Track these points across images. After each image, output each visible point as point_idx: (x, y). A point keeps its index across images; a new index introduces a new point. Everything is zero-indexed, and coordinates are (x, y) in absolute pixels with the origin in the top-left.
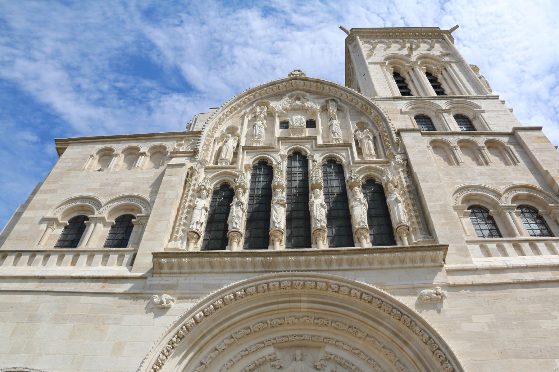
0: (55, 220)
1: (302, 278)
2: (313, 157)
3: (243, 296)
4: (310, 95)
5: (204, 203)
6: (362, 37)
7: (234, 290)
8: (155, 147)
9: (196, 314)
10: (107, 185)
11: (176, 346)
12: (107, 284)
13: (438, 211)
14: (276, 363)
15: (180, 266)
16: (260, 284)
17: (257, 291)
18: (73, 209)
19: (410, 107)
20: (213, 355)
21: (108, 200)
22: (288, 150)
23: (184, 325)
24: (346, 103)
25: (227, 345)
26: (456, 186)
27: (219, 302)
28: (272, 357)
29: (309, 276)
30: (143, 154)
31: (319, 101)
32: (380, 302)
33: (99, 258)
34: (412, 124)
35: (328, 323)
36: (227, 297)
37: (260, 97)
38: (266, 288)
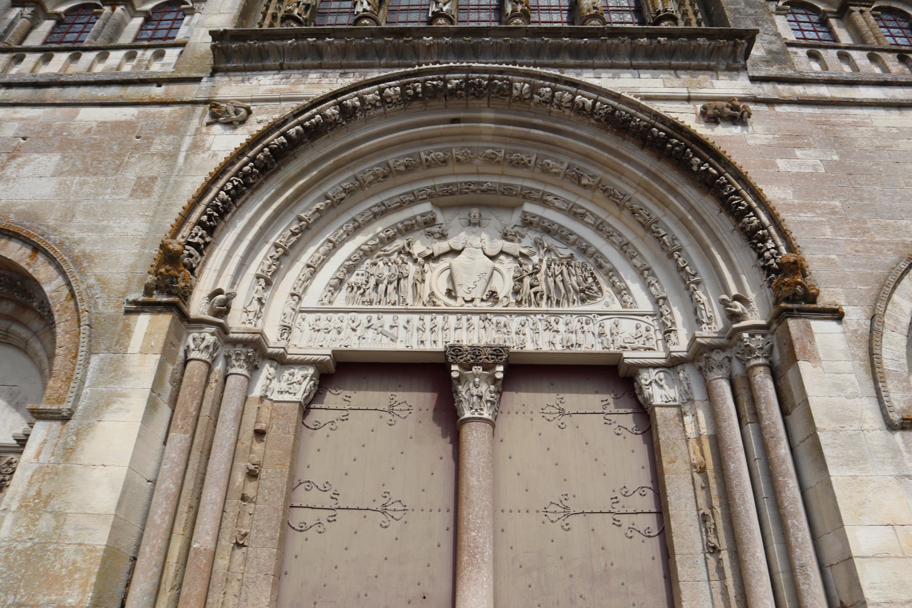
1: (487, 76)
3: (378, 104)
9: (289, 129)
11: (253, 184)
14: (435, 229)
16: (409, 83)
20: (321, 206)
23: (267, 146)
25: (347, 191)
27: (333, 111)
28: (429, 216)
29: (501, 72)
35: (530, 162)
36: (348, 102)
38: (419, 90)
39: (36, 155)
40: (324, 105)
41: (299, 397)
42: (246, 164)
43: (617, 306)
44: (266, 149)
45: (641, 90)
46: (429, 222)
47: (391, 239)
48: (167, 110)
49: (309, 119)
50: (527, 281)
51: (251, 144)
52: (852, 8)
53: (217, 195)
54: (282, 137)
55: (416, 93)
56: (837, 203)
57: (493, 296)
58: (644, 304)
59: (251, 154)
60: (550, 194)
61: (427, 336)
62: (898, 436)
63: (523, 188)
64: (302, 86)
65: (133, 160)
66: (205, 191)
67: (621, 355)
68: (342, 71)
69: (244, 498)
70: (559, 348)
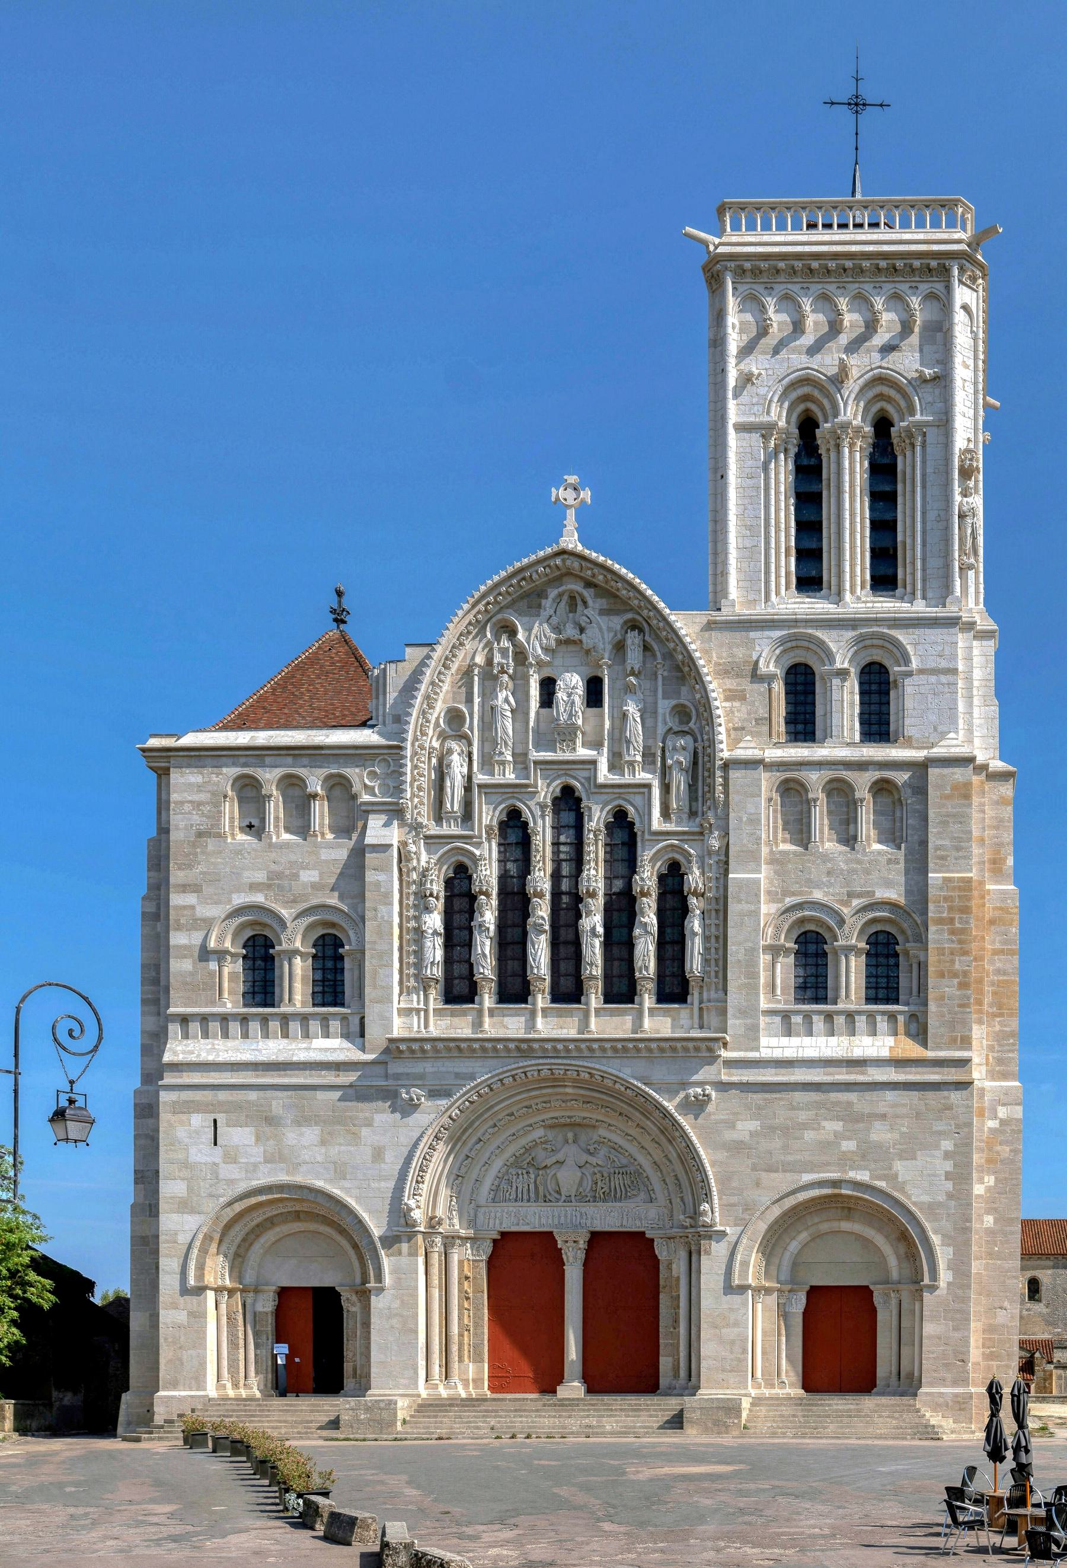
0: (227, 952)
2: (590, 809)
4: (597, 596)
5: (434, 921)
6: (740, 273)
7: (489, 1082)
8: (331, 776)
10: (279, 875)
12: (341, 1073)
13: (739, 961)
15: (423, 1051)
17: (515, 1080)
18: (242, 927)
19: (778, 652)
21: (294, 911)
24: (657, 637)
26: (788, 900)
30: (314, 796)
31: (611, 625)
32: (643, 1100)
33: (315, 1026)
34: (767, 715)
37: (497, 608)
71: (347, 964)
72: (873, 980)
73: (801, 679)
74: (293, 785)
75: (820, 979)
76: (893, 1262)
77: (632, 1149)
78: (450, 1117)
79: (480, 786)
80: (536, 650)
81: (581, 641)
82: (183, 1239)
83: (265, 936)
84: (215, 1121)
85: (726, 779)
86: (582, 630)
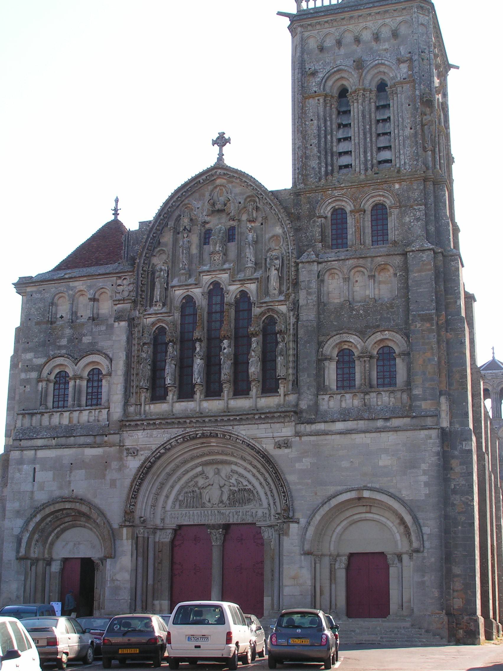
16: (185, 437)
22: (208, 285)
23: (145, 467)
39: (78, 471)
40: (160, 449)
41: (169, 540)
42: (141, 475)
43: (258, 505)
44: (146, 468)
45: (258, 435)
46: (202, 473)
47: (192, 480)
48: (113, 449)
49: (156, 454)
50: (232, 496)
51: (141, 467)
52: (361, 359)
53: (135, 487)
54: (150, 463)
55: (188, 440)
56: (310, 481)
57: (222, 502)
58: (265, 504)
59: (141, 471)
60: (239, 463)
61: (204, 519)
62: (303, 557)
63: (230, 460)
64: (152, 438)
65: (107, 472)
66: (132, 486)
67: (255, 523)
68: (163, 430)
69: (158, 570)
70: (239, 522)
71: (104, 383)
72: (382, 373)
73: (339, 217)
74: (82, 295)
75: (352, 375)
76: (398, 537)
77: (249, 476)
78: (150, 462)
79: (173, 287)
80: (202, 216)
81: (224, 210)
82: (17, 531)
83: (66, 372)
84: (35, 468)
85: (297, 270)
86: (225, 205)
